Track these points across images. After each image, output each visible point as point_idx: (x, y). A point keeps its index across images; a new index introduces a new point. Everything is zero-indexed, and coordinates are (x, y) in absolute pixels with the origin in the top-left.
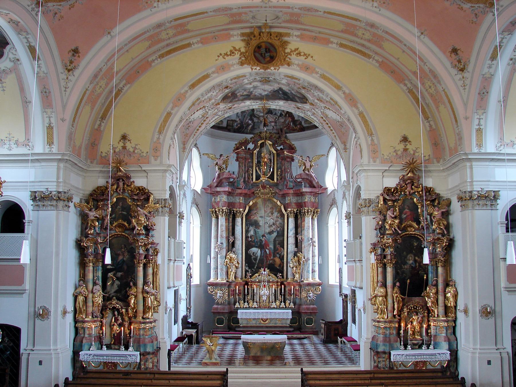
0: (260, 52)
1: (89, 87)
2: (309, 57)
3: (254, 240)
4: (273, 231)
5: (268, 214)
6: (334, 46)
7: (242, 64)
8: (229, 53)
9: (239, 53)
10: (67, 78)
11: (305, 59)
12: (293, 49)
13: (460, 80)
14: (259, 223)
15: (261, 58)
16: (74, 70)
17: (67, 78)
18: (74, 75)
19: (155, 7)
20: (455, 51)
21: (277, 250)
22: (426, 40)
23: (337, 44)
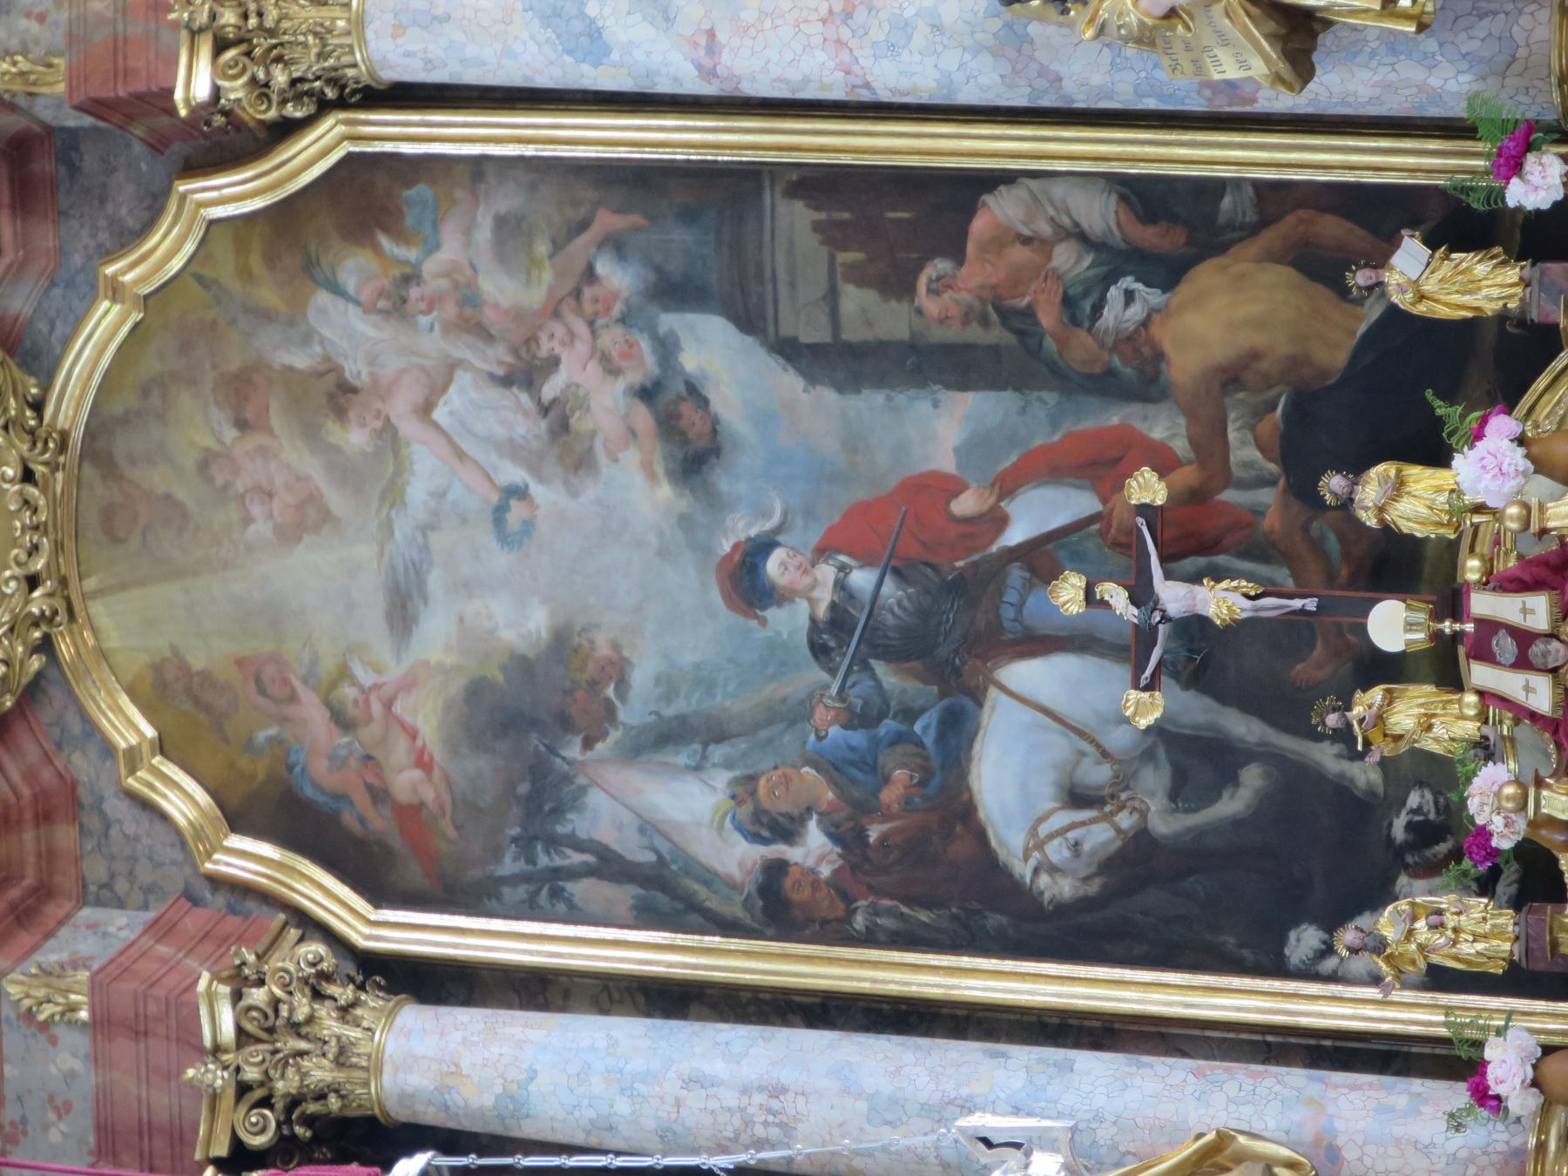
3: (832, 766)
4: (647, 393)
5: (346, 472)
14: (523, 667)
21: (1021, 322)
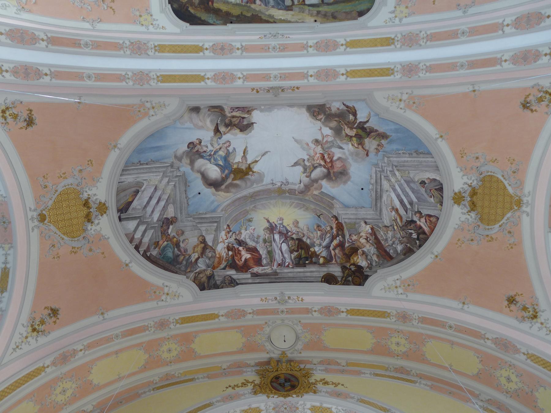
0: (279, 382)
1: (48, 367)
2: (340, 386)
6: (368, 375)
7: (255, 393)
8: (240, 385)
9: (253, 385)
10: (26, 337)
11: (335, 387)
12: (318, 380)
13: (540, 329)
15: (279, 387)
16: (40, 333)
17: (26, 337)
18: (37, 340)
19: (163, 300)
20: (511, 300)
22: (473, 308)
23: (370, 374)
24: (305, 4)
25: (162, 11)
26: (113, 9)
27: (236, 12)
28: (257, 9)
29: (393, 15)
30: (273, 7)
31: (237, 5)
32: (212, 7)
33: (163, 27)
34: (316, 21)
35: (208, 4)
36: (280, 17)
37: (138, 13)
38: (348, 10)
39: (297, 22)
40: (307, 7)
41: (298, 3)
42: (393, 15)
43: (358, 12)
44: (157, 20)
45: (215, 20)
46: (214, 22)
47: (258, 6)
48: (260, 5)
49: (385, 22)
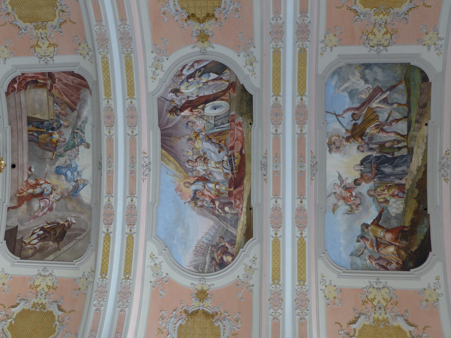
24: (407, 135)
25: (417, 278)
26: (425, 327)
27: (414, 204)
28: (411, 183)
29: (433, 47)
30: (408, 167)
31: (406, 203)
32: (409, 228)
33: (436, 279)
34: (426, 124)
35: (406, 231)
36: (420, 160)
37: (425, 303)
38: (419, 92)
39: (426, 143)
40: (411, 133)
41: (406, 142)
42: (433, 47)
43: (422, 83)
44: (429, 284)
45: (424, 226)
46: (426, 226)
47: (408, 182)
48: (406, 179)
49: (438, 55)
